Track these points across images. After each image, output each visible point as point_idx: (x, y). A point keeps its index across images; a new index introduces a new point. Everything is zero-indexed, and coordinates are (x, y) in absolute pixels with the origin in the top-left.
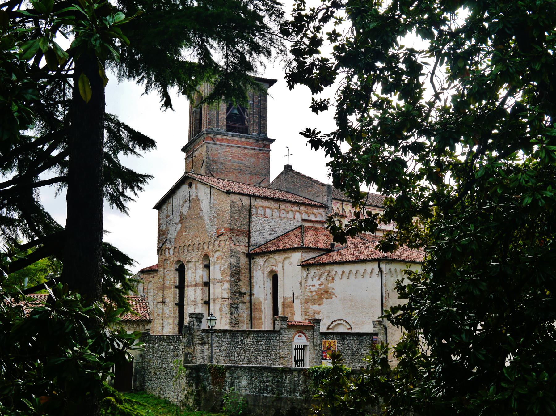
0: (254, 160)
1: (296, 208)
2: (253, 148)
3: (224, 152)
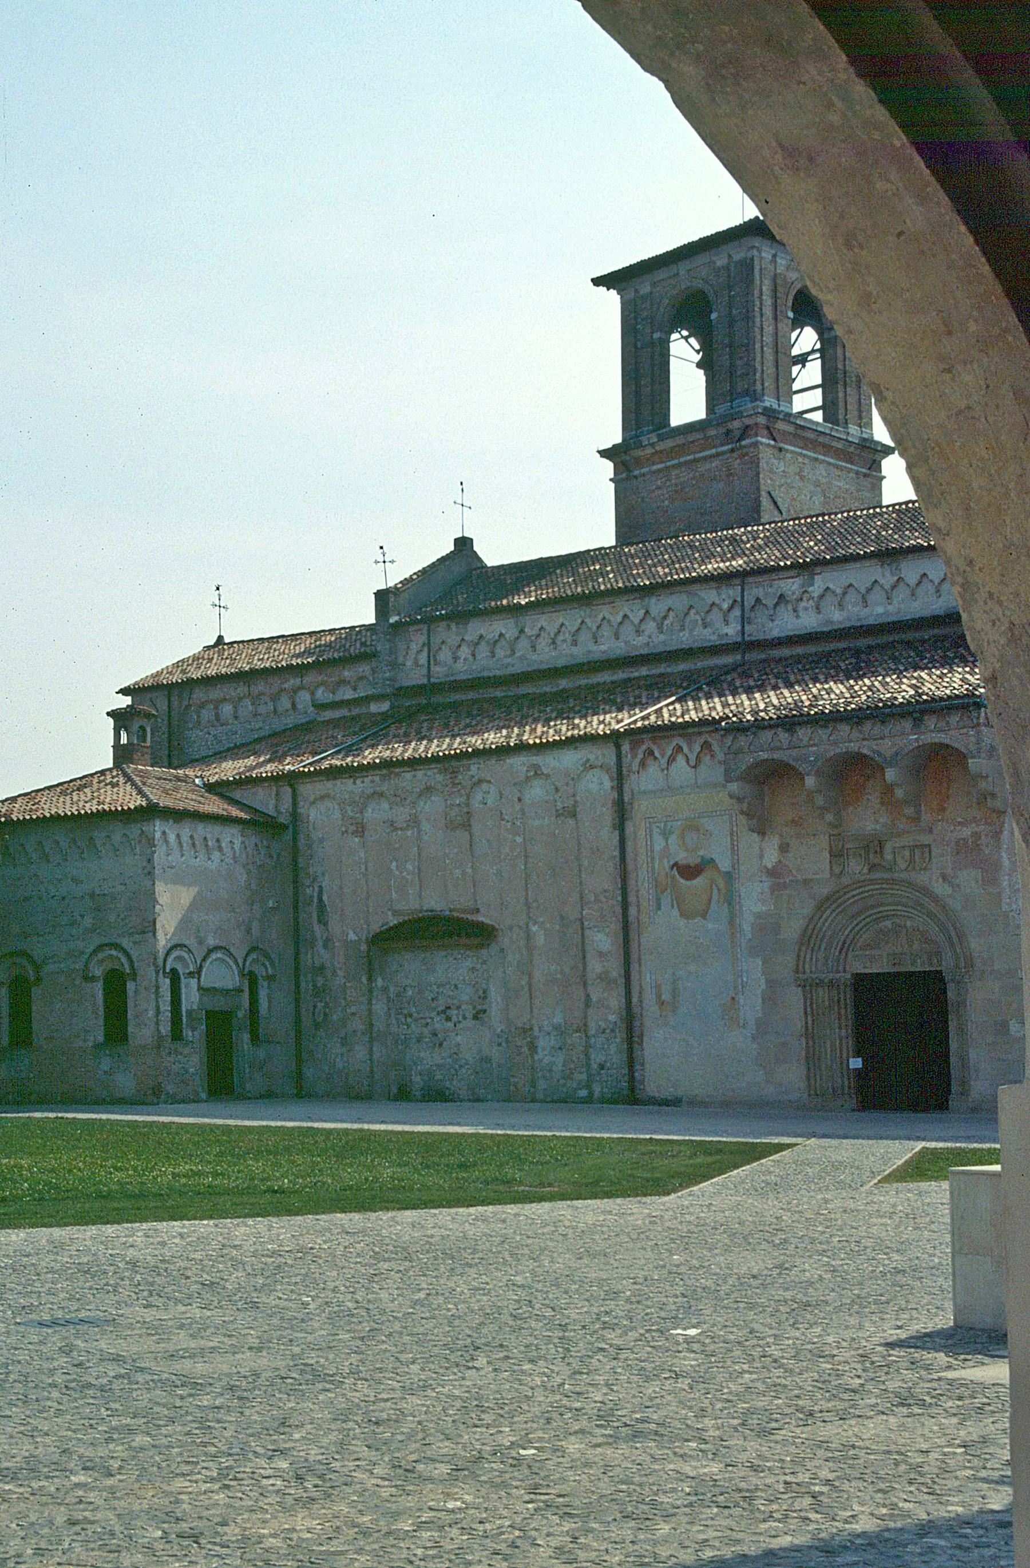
0: (721, 485)
1: (294, 682)
2: (714, 451)
3: (653, 491)
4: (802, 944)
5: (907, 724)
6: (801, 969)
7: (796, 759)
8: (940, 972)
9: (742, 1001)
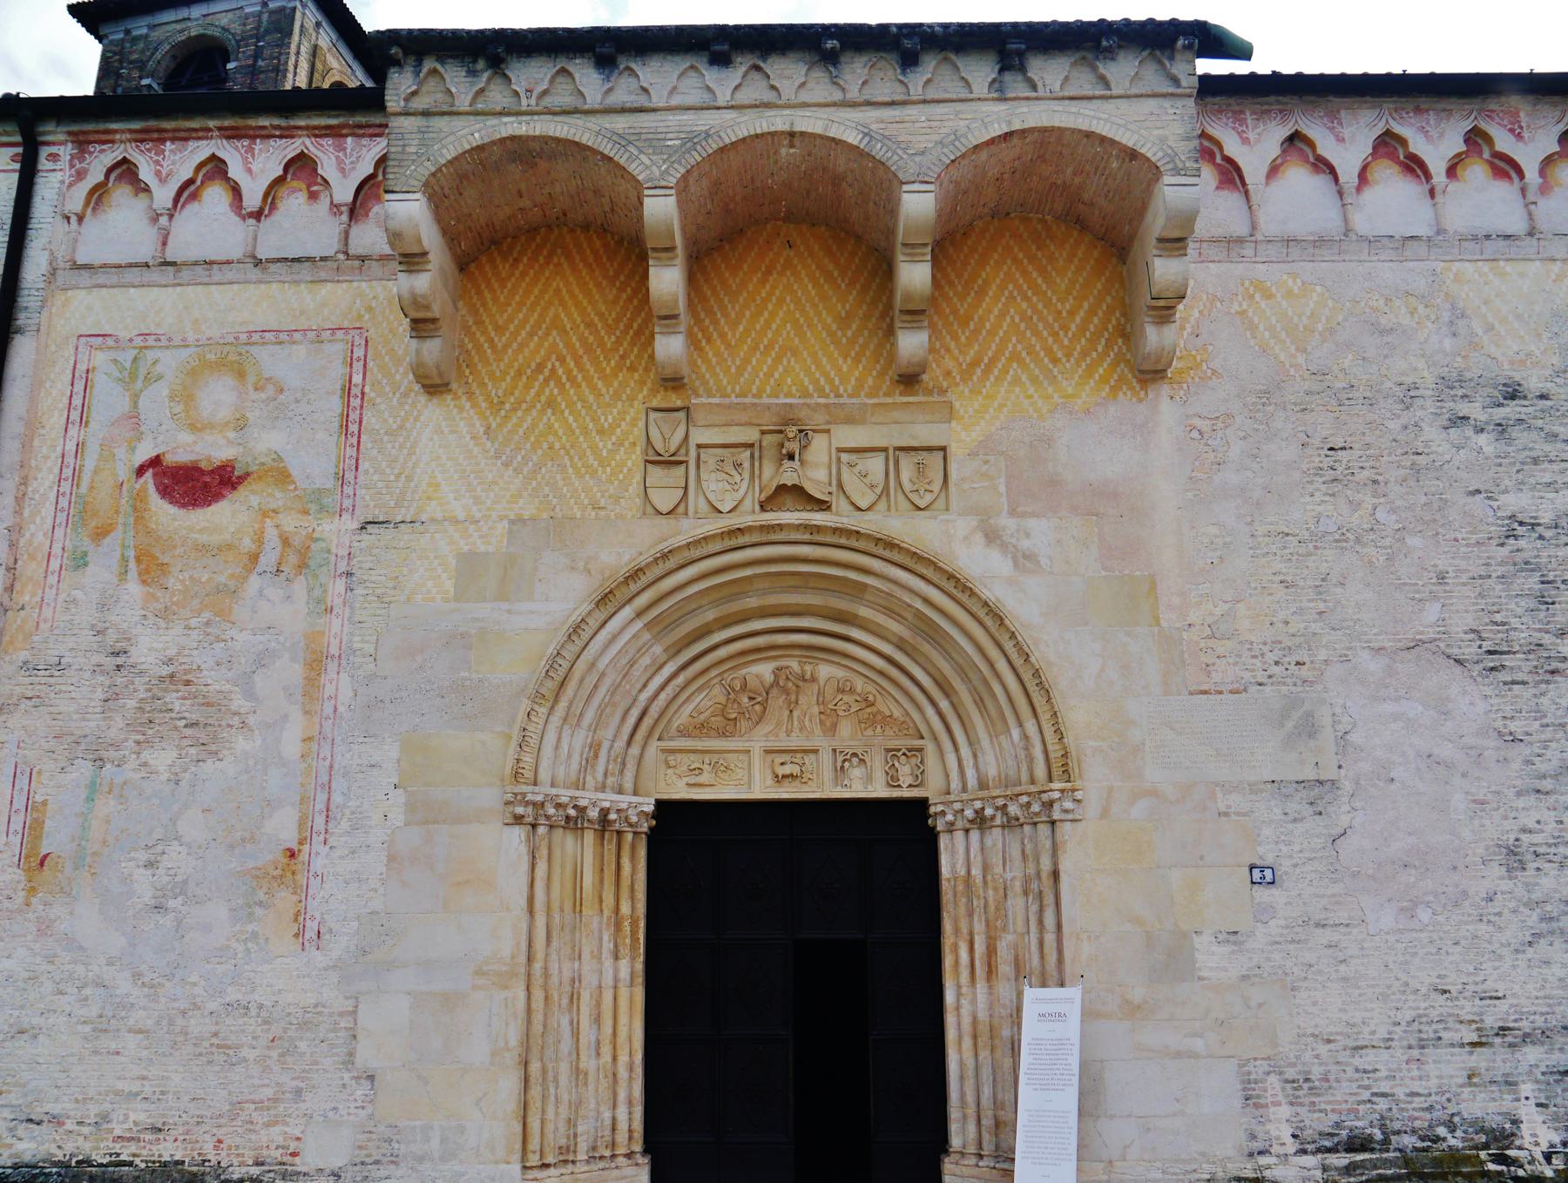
4: (538, 696)
5: (980, 71)
6: (528, 774)
7: (623, 140)
8: (923, 804)
9: (318, 864)
